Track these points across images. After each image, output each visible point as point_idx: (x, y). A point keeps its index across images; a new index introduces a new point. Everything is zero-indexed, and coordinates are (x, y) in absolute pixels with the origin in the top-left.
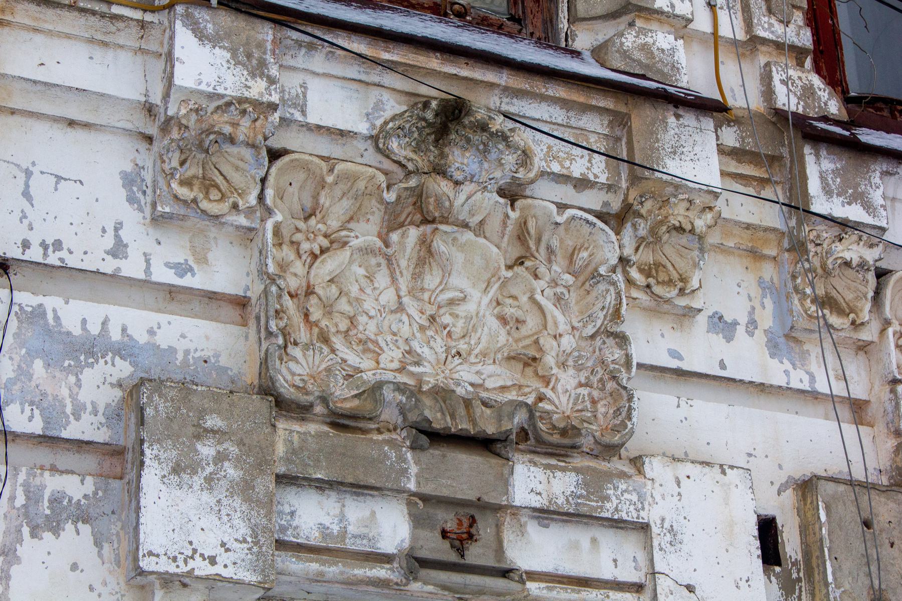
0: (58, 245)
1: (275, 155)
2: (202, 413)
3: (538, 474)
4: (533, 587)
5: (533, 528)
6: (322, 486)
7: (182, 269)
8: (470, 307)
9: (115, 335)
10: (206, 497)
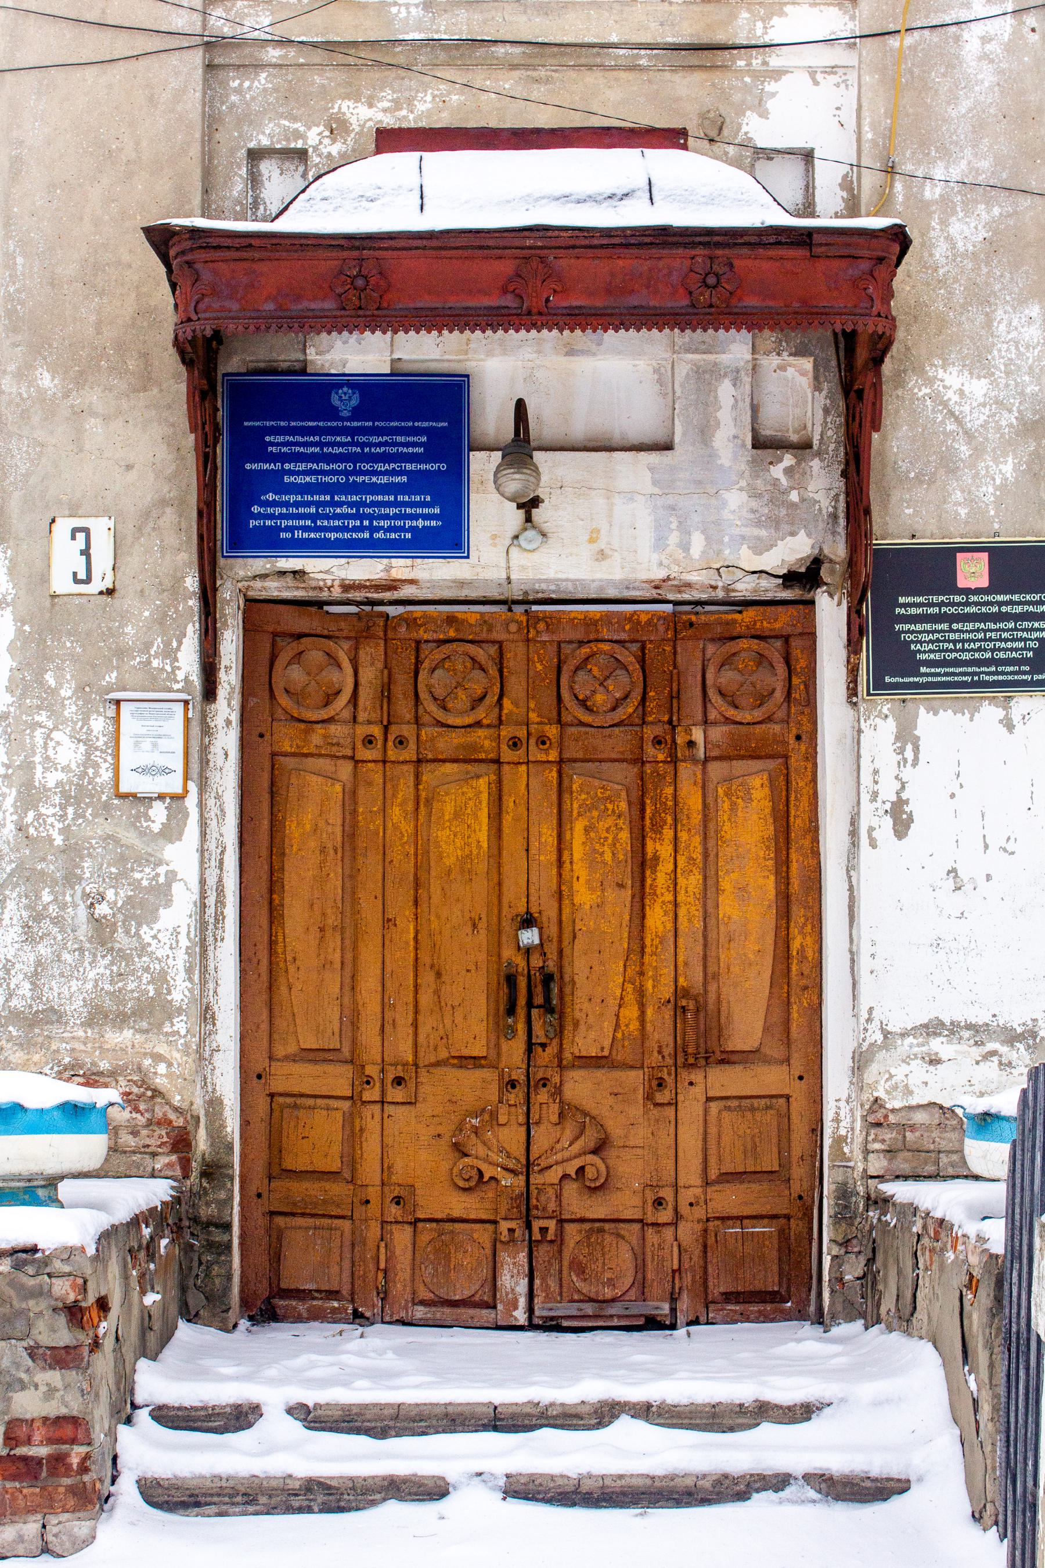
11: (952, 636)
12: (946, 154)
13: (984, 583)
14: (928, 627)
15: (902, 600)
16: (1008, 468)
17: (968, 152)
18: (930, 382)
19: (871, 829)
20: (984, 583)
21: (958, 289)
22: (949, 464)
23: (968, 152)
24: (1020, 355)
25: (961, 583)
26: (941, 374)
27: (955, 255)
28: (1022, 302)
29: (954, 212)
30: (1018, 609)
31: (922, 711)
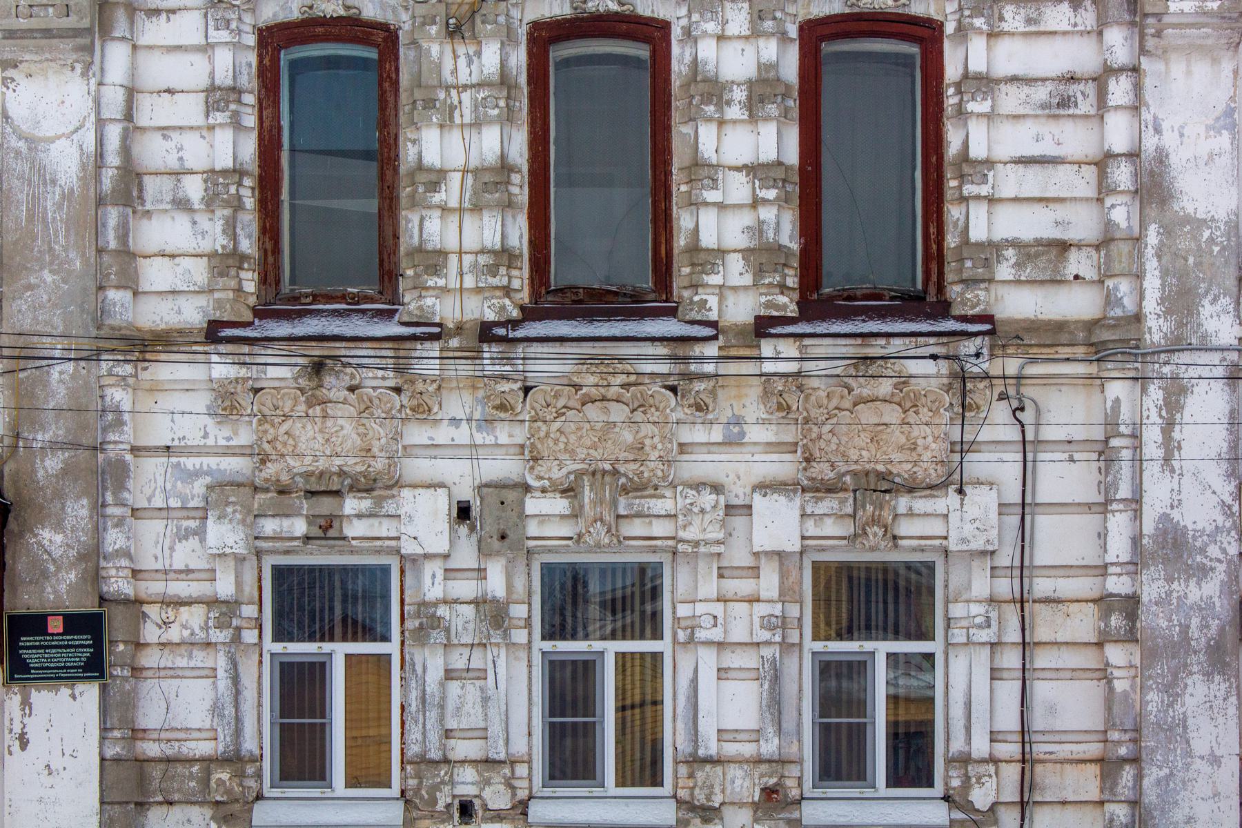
0: (184, 438)
1: (257, 391)
2: (228, 497)
3: (356, 501)
4: (354, 543)
5: (355, 521)
6: (273, 516)
7: (229, 439)
8: (345, 432)
9: (205, 468)
10: (230, 526)
11: (46, 656)
12: (44, 429)
13: (61, 630)
14: (35, 651)
15: (22, 639)
16: (72, 576)
17: (53, 427)
18: (36, 536)
19: (9, 746)
20: (61, 630)
21: (49, 492)
22: (45, 574)
23: (53, 427)
24: (78, 522)
25: (50, 631)
26: (41, 532)
27: (47, 476)
28: (78, 498)
29: (47, 456)
30: (76, 643)
31: (33, 690)
